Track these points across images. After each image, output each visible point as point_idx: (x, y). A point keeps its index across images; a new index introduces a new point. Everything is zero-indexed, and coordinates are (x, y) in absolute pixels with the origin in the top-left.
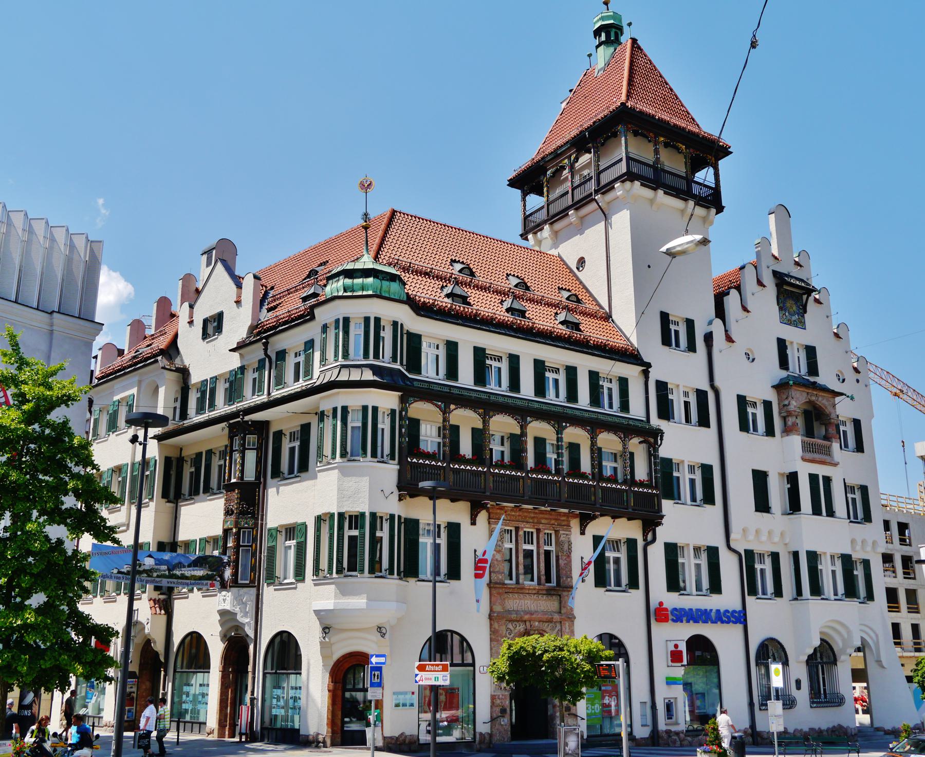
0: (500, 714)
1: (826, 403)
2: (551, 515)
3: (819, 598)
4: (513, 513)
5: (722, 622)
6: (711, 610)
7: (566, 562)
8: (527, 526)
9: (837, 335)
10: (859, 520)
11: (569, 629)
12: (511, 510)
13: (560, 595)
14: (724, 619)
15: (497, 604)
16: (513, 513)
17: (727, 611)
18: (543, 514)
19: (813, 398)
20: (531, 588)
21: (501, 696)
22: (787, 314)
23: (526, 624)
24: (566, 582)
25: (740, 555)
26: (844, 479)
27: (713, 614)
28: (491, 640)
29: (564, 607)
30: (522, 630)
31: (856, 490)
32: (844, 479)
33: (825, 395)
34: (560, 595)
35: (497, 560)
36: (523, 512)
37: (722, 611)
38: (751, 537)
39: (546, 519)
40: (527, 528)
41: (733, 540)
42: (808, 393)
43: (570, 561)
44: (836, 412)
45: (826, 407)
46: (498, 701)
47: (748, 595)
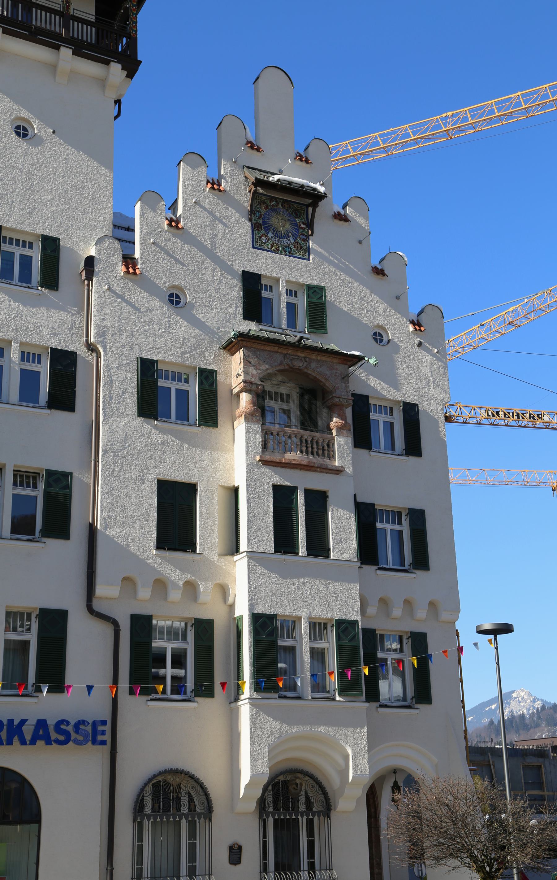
1: (328, 373)
3: (276, 695)
5: (49, 742)
6: (23, 722)
9: (379, 272)
10: (407, 567)
14: (54, 735)
17: (82, 722)
19: (298, 364)
22: (270, 235)
25: (115, 624)
26: (355, 495)
27: (28, 731)
31: (404, 518)
32: (355, 495)
33: (323, 358)
37: (51, 723)
38: (144, 593)
41: (100, 598)
42: (285, 356)
44: (347, 387)
45: (327, 379)
47: (132, 692)
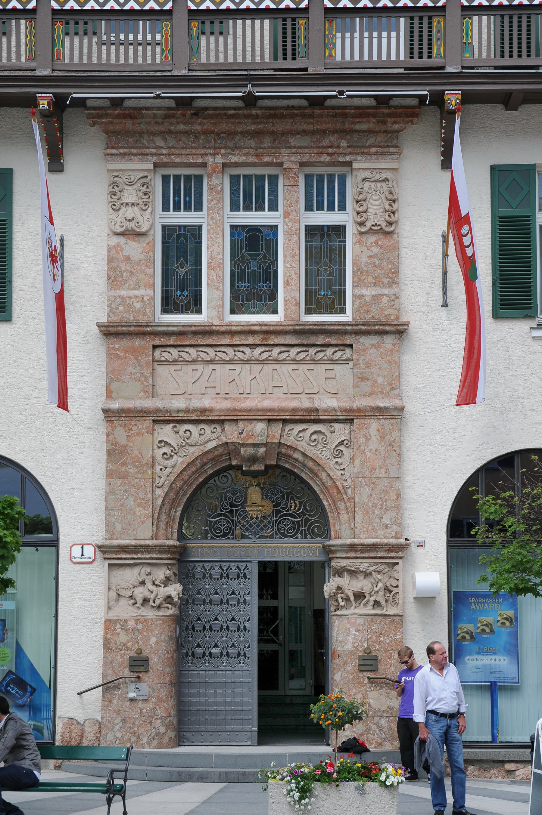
0: (126, 673)
2: (311, 116)
4: (182, 127)
7: (375, 250)
8: (235, 159)
11: (382, 438)
12: (166, 117)
13: (351, 346)
15: (125, 378)
16: (182, 127)
18: (283, 116)
20: (234, 328)
21: (132, 623)
23: (223, 430)
24: (374, 308)
28: (110, 474)
29: (363, 379)
30: (211, 445)
34: (351, 346)
35: (128, 259)
36: (211, 117)
39: (305, 133)
40: (237, 165)
43: (395, 248)
46: (123, 637)
